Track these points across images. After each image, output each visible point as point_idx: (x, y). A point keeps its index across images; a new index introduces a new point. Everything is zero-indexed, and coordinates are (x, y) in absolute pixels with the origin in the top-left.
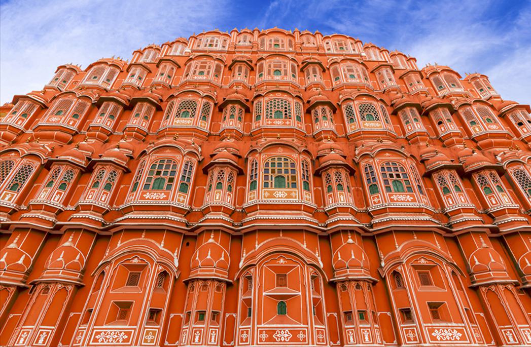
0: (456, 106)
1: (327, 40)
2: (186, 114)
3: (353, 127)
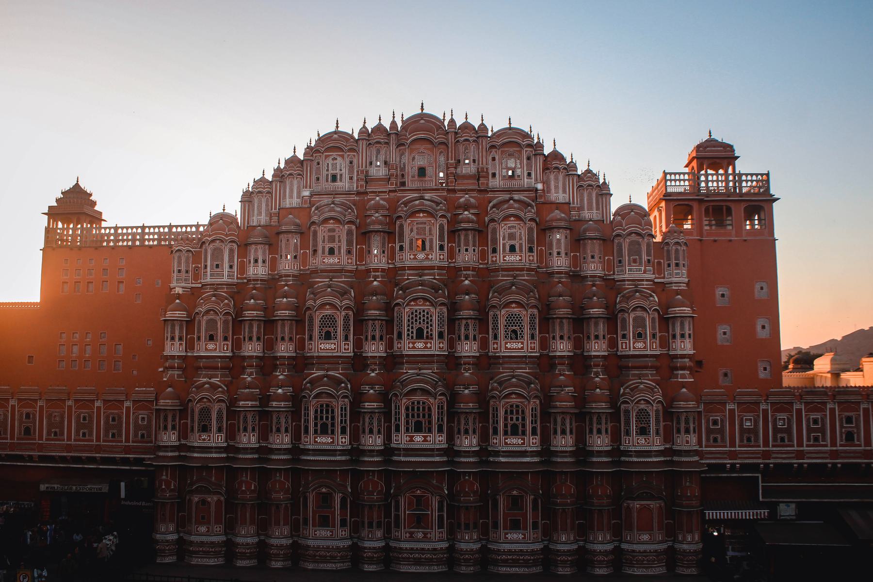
0: (618, 306)
1: (494, 153)
2: (328, 336)
3: (495, 346)
